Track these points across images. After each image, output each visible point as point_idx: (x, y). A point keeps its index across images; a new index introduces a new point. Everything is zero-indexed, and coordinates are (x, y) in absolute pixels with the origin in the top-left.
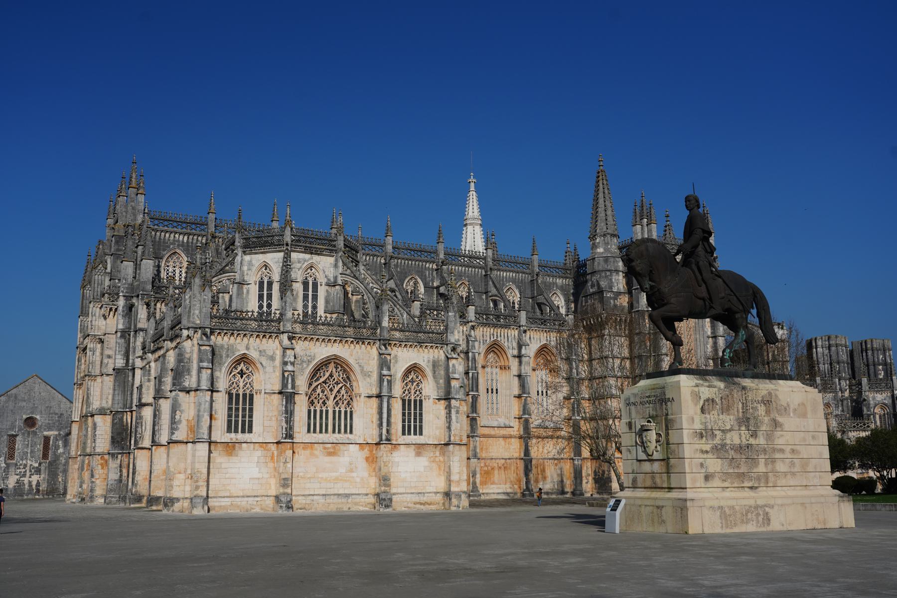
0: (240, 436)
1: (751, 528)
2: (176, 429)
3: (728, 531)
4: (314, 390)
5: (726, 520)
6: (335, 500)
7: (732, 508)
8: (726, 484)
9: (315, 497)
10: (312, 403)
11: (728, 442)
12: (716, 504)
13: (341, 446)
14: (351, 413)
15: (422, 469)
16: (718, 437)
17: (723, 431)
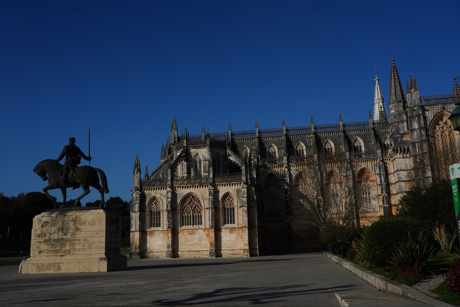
0: (155, 228)
1: (51, 272)
2: (132, 227)
4: (185, 208)
5: (39, 268)
6: (193, 253)
7: (43, 264)
8: (49, 255)
9: (185, 252)
10: (184, 213)
11: (52, 238)
12: (35, 262)
13: (196, 231)
14: (201, 216)
15: (233, 239)
16: (47, 236)
17: (51, 234)
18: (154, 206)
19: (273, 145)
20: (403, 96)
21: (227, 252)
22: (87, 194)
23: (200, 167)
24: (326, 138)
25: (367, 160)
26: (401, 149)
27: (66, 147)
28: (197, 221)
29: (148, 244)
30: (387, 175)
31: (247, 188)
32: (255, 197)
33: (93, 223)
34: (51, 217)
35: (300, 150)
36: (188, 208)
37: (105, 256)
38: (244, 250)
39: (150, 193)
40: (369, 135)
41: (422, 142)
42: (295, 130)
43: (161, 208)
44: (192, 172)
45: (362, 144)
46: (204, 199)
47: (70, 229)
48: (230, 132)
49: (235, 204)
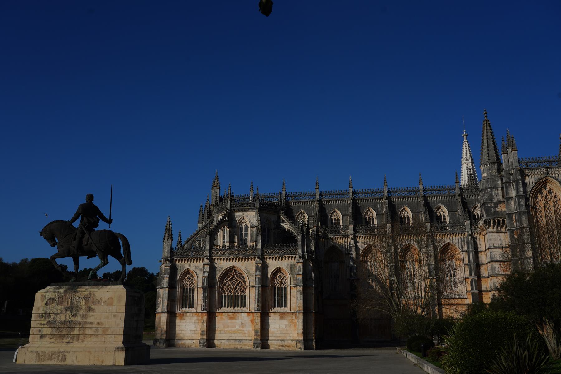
0: (187, 310)
1: (53, 362)
2: (159, 307)
3: (39, 363)
4: (225, 285)
6: (233, 342)
7: (44, 352)
8: (52, 340)
10: (224, 291)
11: (58, 319)
12: (35, 350)
13: (238, 314)
14: (245, 296)
15: (284, 327)
16: (52, 317)
17: (56, 314)
18: (187, 281)
19: (336, 210)
20: (497, 156)
21: (275, 342)
22: (104, 265)
23: (246, 235)
24: (402, 204)
25: (452, 233)
26: (494, 222)
27: (82, 206)
28: (240, 302)
29: (177, 329)
30: (477, 253)
31: (303, 263)
32: (313, 275)
33: (110, 302)
34: (58, 292)
35: (369, 219)
36: (229, 285)
37: (122, 345)
38: (297, 341)
39: (183, 265)
40: (455, 202)
41: (520, 213)
42: (364, 193)
43: (196, 285)
44: (236, 240)
45: (447, 213)
46: (249, 275)
47: (81, 309)
48: (284, 192)
49: (288, 282)
